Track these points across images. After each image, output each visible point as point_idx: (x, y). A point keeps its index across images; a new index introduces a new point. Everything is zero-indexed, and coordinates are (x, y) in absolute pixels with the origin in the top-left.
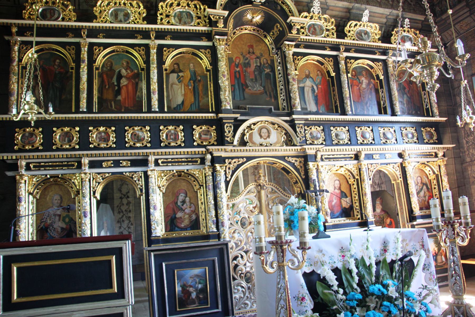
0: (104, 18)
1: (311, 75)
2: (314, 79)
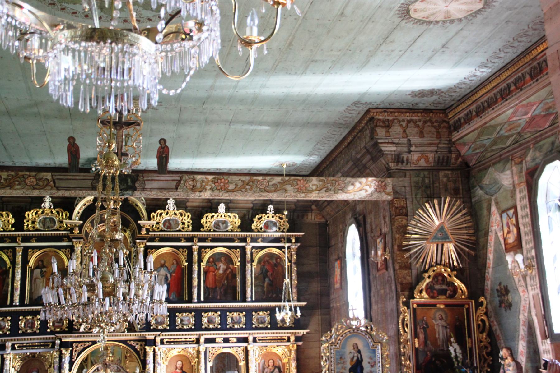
1: (166, 265)
2: (169, 268)
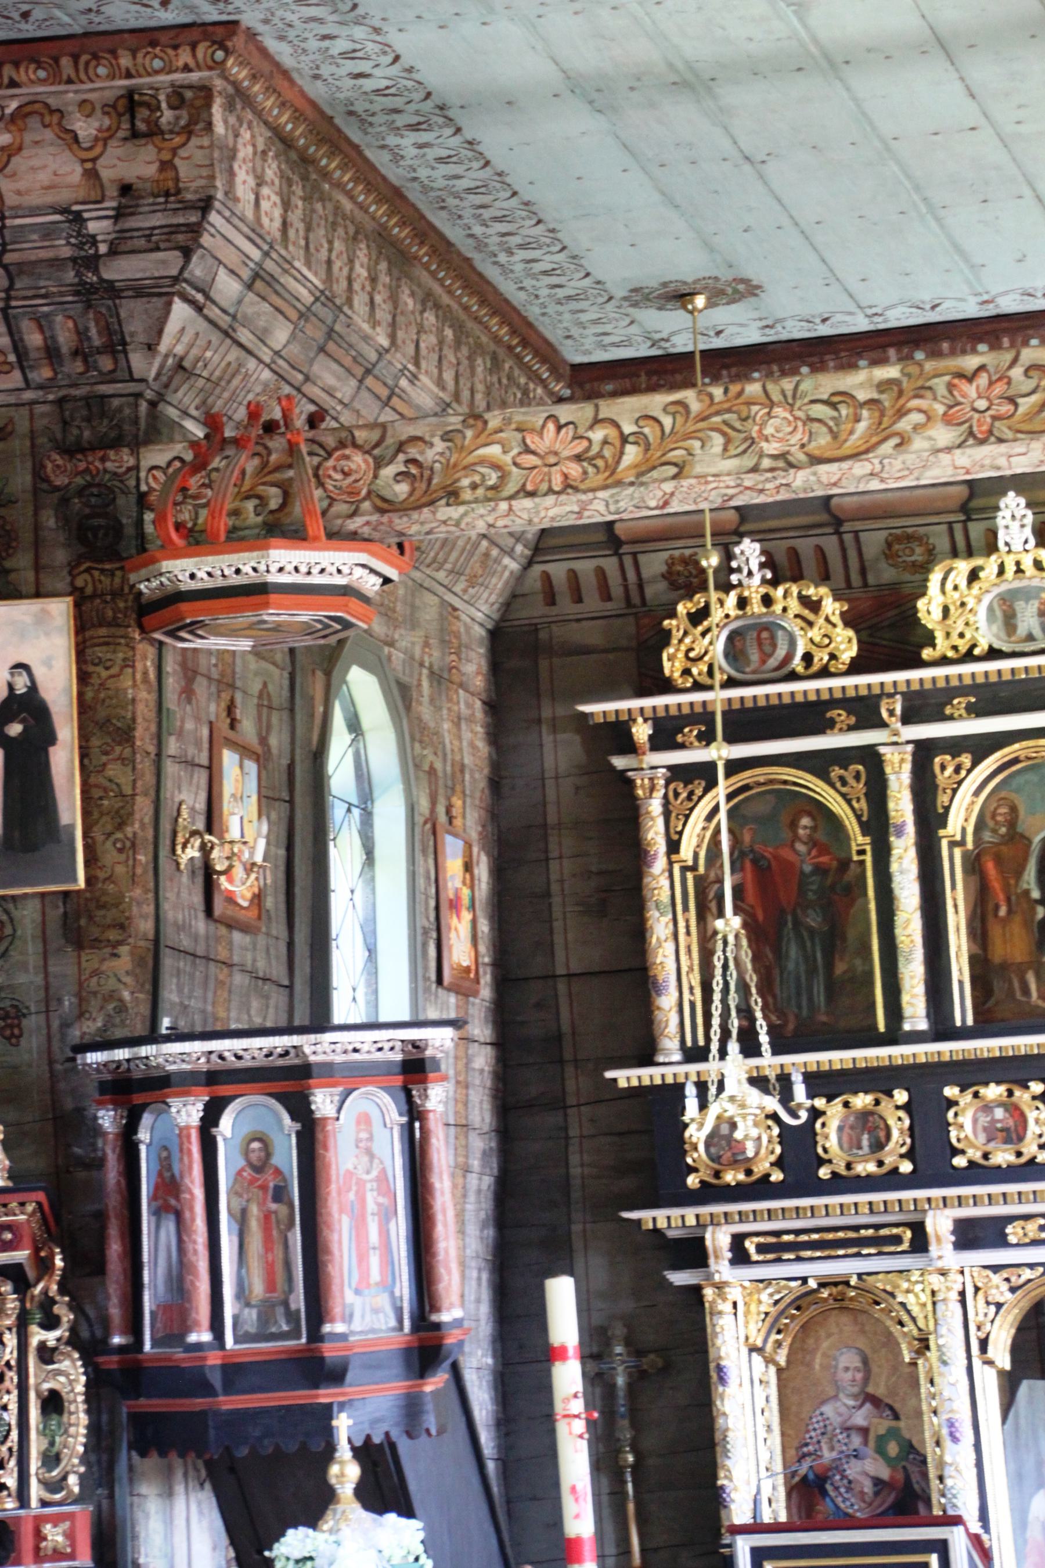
0: (962, 635)
